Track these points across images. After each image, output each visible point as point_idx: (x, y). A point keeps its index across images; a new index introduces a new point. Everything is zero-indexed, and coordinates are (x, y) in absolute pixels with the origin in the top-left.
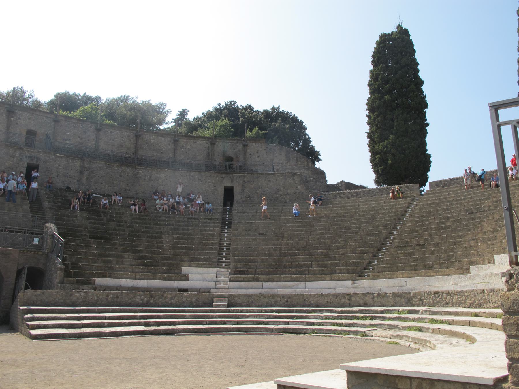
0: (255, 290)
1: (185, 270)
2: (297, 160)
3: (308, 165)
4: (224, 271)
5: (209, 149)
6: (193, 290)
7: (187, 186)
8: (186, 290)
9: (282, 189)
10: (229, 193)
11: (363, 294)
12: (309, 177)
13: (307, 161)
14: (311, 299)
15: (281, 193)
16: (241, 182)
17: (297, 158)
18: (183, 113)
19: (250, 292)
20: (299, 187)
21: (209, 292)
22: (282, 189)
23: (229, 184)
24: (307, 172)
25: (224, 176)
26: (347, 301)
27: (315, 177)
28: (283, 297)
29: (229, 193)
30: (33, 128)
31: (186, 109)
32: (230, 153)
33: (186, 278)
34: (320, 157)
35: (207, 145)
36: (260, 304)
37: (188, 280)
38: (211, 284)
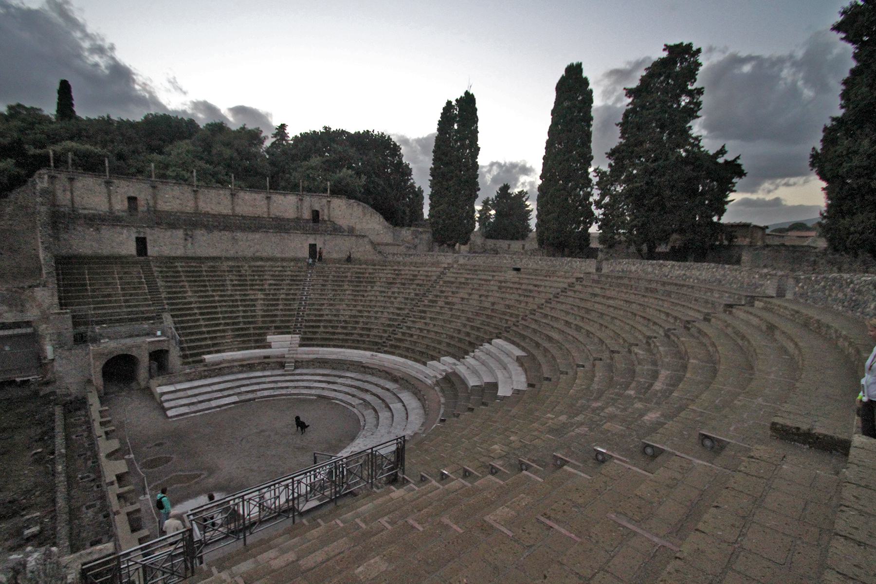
23: (313, 243)
30: (133, 195)
32: (317, 207)
33: (270, 347)
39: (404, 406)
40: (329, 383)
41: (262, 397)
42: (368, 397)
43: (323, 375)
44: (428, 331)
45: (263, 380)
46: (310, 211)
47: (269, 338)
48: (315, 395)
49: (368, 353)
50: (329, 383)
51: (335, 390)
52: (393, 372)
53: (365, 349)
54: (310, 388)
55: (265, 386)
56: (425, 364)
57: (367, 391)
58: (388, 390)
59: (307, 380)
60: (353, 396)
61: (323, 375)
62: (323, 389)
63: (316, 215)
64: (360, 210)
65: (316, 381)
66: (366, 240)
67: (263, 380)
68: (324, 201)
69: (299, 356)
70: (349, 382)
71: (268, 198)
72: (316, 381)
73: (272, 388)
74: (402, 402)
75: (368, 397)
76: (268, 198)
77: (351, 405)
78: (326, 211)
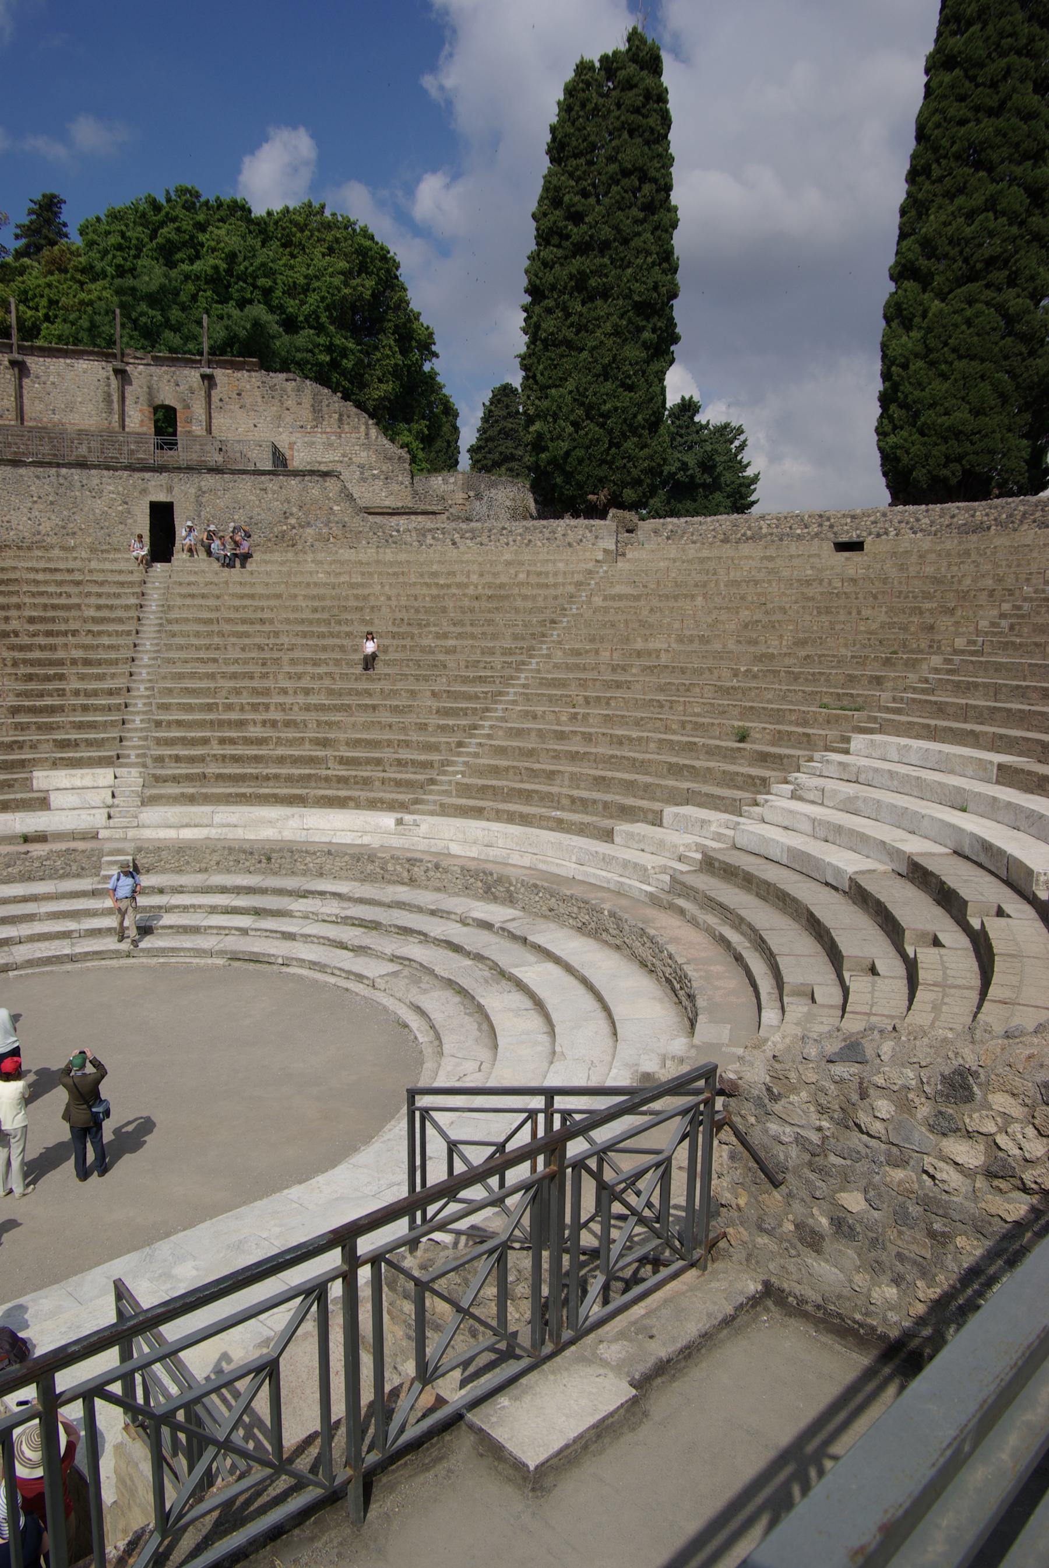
0: (196, 830)
1: (43, 779)
2: (340, 420)
3: (367, 434)
4: (132, 777)
5: (109, 385)
6: (60, 836)
7: (52, 503)
8: (41, 838)
9: (295, 510)
10: (162, 517)
11: (409, 860)
12: (371, 468)
13: (367, 424)
14: (308, 859)
15: (293, 521)
16: (193, 491)
17: (341, 415)
18: (48, 209)
19: (187, 834)
20: (336, 508)
21: (95, 837)
22: (295, 510)
23: (162, 497)
24: (364, 454)
25: (147, 475)
26: (378, 870)
27: (384, 468)
28: (251, 853)
29: (162, 517)
31: (54, 196)
32: (168, 397)
33: (43, 803)
34: (433, 348)
35: (103, 374)
36: (203, 865)
37: (49, 809)
38: (98, 818)
39: (569, 969)
40: (258, 912)
41: (30, 963)
42: (415, 950)
43: (238, 890)
44: (588, 738)
45: (30, 908)
46: (148, 411)
47: (43, 779)
48: (221, 953)
49: (387, 820)
50: (258, 912)
51: (290, 936)
52: (489, 867)
53: (373, 805)
54: (194, 930)
55: (39, 928)
56: (608, 836)
57: (406, 931)
58: (487, 926)
59: (185, 908)
60: (360, 950)
61: (238, 890)
62: (244, 932)
63: (165, 421)
64: (307, 400)
65: (213, 910)
66: (331, 483)
67: (30, 908)
68: (192, 376)
69: (147, 834)
70: (332, 908)
71: (21, 369)
72: (213, 910)
73: (66, 935)
74: (557, 960)
75: (415, 950)
76: (21, 369)
77: (360, 977)
78: (198, 409)
